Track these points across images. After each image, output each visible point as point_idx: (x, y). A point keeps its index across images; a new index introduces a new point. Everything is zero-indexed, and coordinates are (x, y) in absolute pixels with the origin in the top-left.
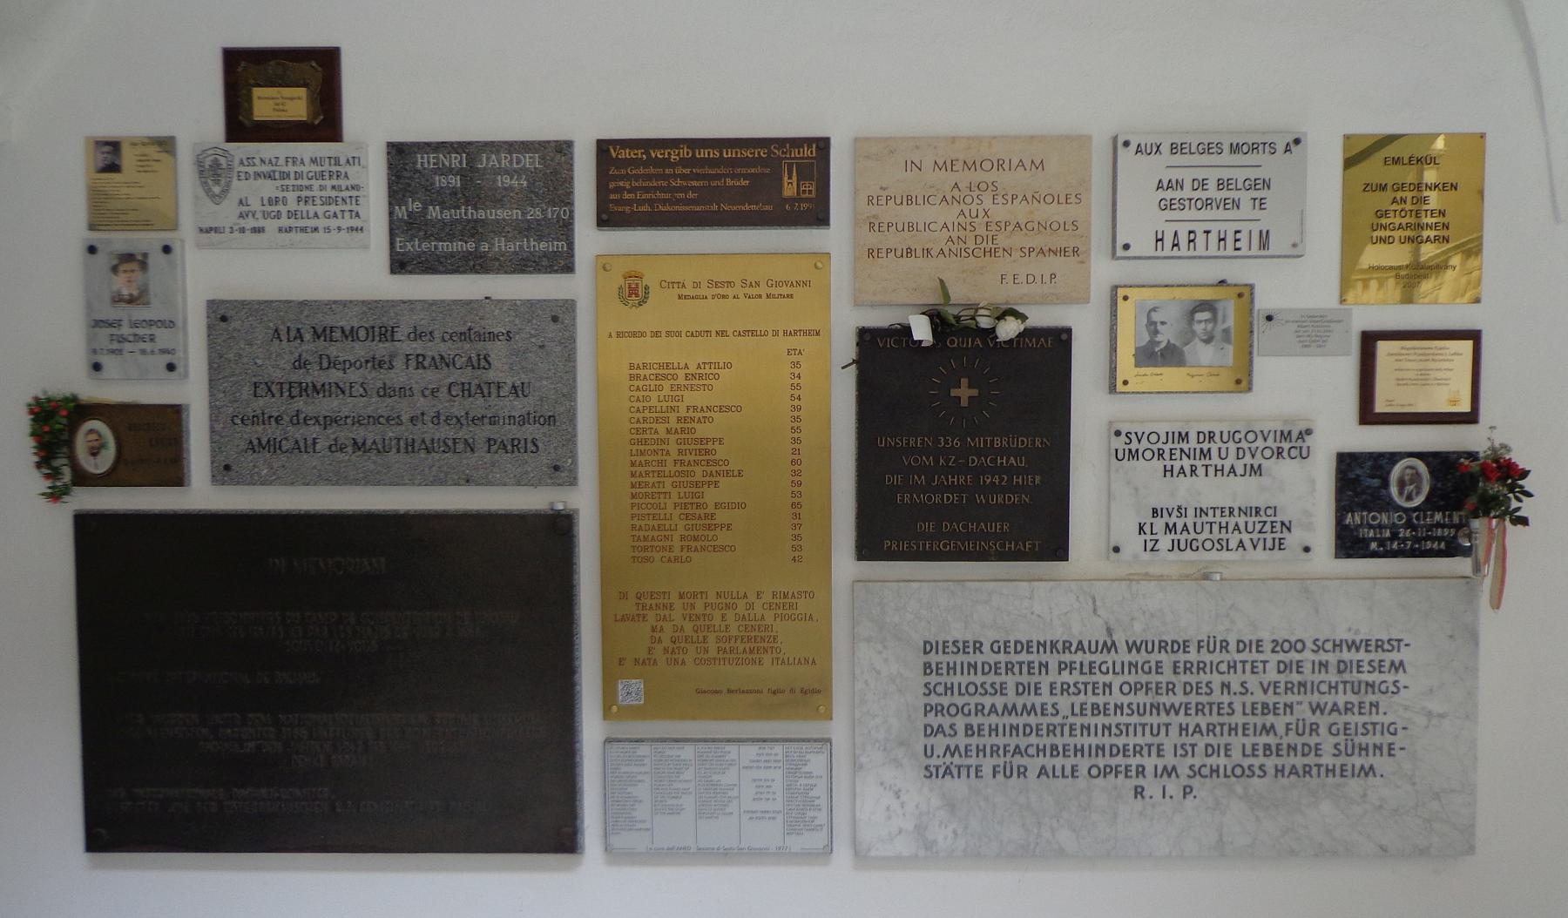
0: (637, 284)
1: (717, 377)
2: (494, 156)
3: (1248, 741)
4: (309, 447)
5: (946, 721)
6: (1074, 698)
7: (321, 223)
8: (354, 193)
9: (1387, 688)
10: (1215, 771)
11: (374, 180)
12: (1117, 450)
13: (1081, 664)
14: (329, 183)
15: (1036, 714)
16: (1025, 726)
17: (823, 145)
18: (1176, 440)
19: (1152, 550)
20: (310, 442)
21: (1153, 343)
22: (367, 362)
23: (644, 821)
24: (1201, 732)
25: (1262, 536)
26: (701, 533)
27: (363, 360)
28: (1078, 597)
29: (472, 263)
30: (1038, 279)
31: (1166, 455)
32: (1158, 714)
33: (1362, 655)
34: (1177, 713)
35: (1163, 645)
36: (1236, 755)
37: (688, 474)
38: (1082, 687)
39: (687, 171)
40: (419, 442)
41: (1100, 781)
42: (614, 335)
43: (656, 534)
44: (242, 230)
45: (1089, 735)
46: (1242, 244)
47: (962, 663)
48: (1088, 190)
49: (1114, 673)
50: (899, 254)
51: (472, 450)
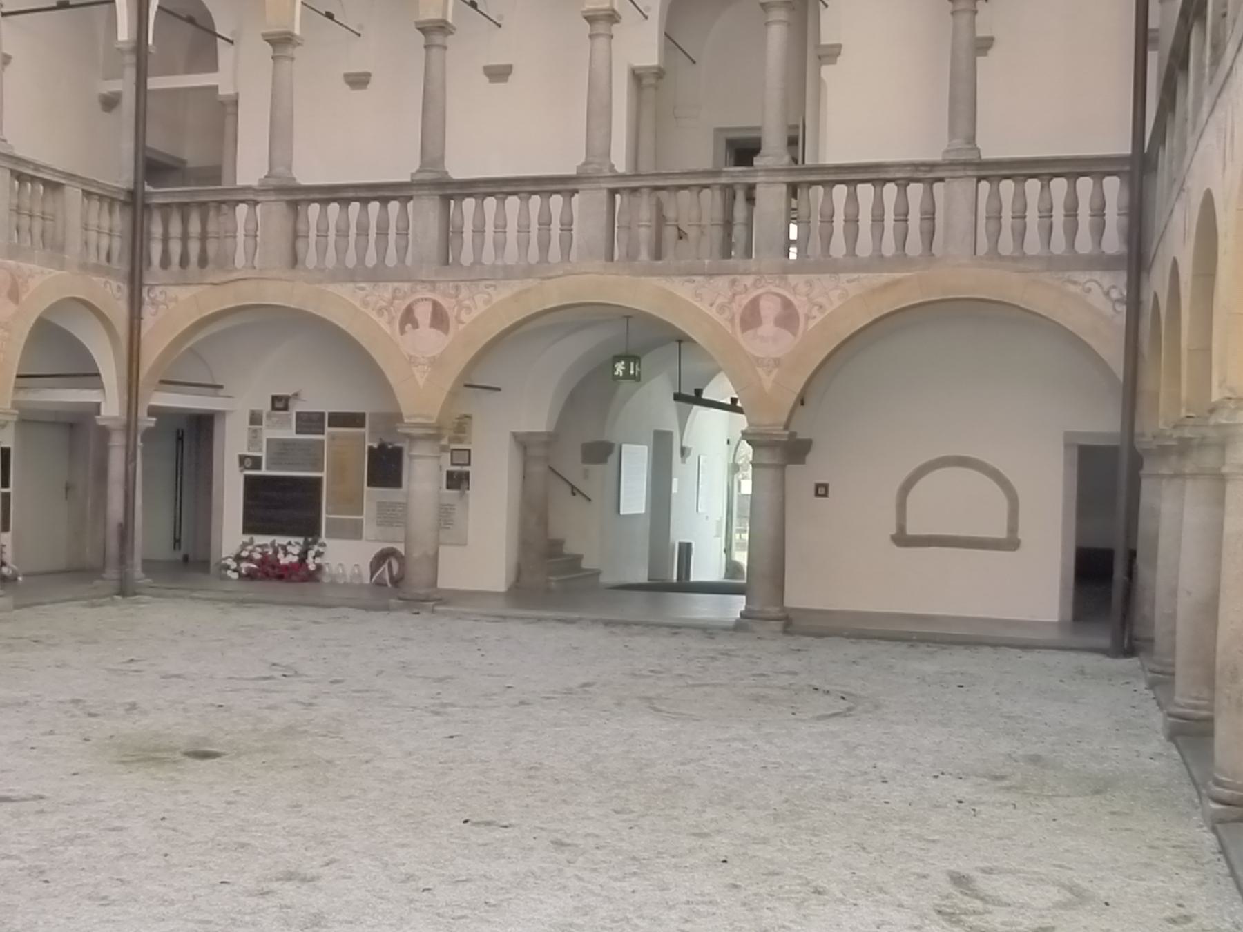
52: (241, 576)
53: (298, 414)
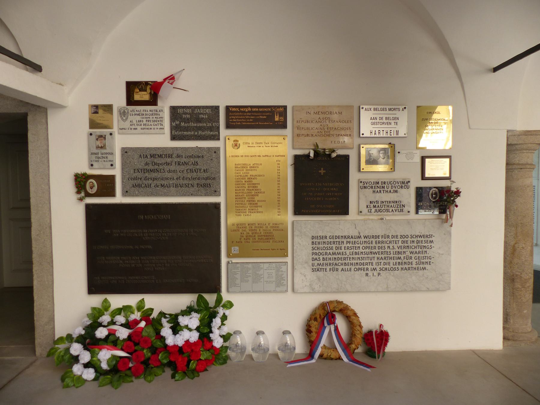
0: (237, 143)
2: (199, 110)
3: (394, 261)
4: (149, 186)
5: (317, 257)
7: (152, 127)
8: (161, 119)
10: (386, 269)
11: (166, 116)
12: (361, 186)
14: (154, 117)
15: (341, 255)
16: (338, 258)
17: (285, 107)
18: (376, 184)
19: (370, 212)
21: (370, 159)
22: (165, 163)
24: (382, 259)
26: (254, 208)
27: (164, 163)
28: (351, 224)
29: (193, 138)
31: (373, 188)
32: (372, 254)
33: (423, 239)
34: (376, 254)
35: (373, 237)
37: (250, 193)
40: (179, 184)
42: (231, 156)
43: (242, 208)
44: (131, 129)
45: (354, 260)
46: (392, 134)
48: (353, 119)
49: (361, 244)
50: (305, 136)
51: (193, 187)
52: (99, 372)
53: (174, 110)
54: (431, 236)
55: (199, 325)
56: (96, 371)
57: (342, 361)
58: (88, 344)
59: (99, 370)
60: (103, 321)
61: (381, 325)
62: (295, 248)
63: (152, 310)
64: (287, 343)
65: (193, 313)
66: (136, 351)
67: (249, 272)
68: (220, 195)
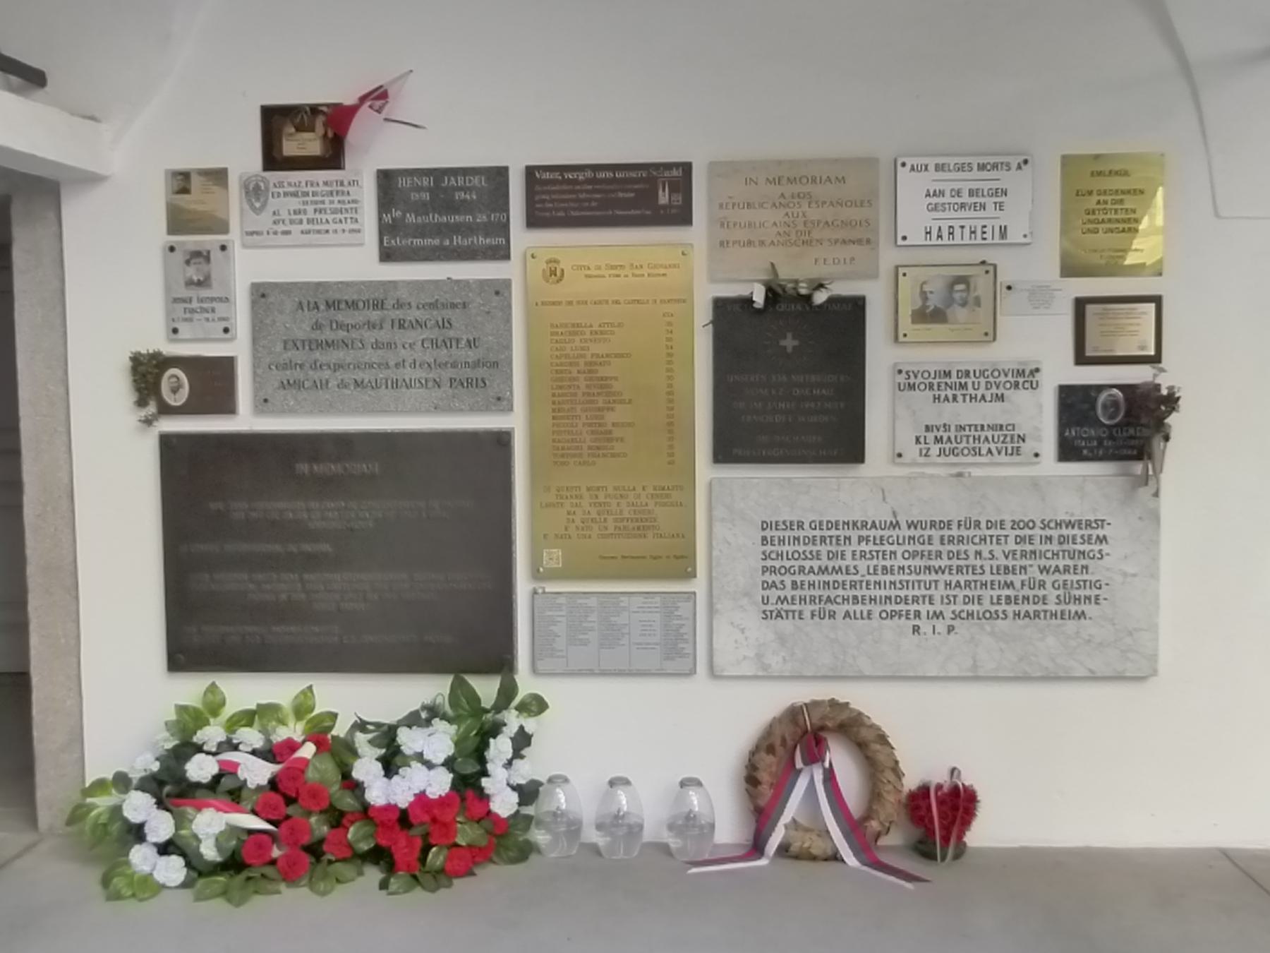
0: (556, 268)
1: (613, 333)
3: (995, 593)
4: (324, 385)
5: (777, 578)
6: (869, 562)
7: (331, 227)
8: (354, 205)
9: (1094, 555)
10: (970, 615)
13: (874, 538)
14: (336, 199)
17: (687, 168)
20: (324, 382)
21: (924, 307)
22: (364, 324)
23: (561, 651)
24: (960, 587)
25: (1004, 445)
29: (437, 254)
30: (842, 261)
31: (935, 387)
33: (1076, 531)
34: (943, 572)
35: (933, 524)
36: (986, 604)
38: (875, 554)
39: (590, 187)
41: (888, 622)
42: (540, 304)
44: (275, 233)
47: (789, 537)
51: (439, 386)
52: (198, 869)
53: (386, 179)
54: (1101, 523)
55: (454, 754)
56: (188, 865)
57: (840, 865)
58: (168, 796)
59: (195, 862)
60: (206, 739)
61: (953, 770)
62: (715, 553)
63: (334, 716)
64: (691, 811)
65: (436, 721)
66: (288, 817)
67: (589, 619)
68: (511, 409)
